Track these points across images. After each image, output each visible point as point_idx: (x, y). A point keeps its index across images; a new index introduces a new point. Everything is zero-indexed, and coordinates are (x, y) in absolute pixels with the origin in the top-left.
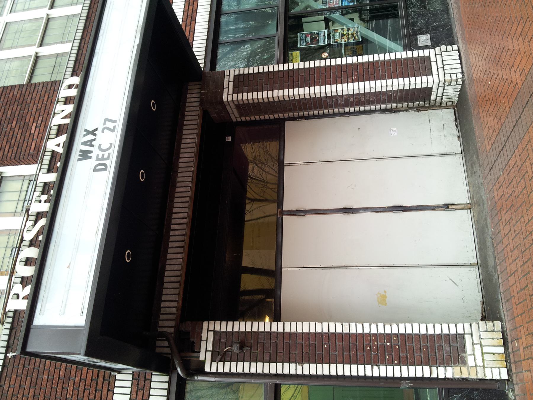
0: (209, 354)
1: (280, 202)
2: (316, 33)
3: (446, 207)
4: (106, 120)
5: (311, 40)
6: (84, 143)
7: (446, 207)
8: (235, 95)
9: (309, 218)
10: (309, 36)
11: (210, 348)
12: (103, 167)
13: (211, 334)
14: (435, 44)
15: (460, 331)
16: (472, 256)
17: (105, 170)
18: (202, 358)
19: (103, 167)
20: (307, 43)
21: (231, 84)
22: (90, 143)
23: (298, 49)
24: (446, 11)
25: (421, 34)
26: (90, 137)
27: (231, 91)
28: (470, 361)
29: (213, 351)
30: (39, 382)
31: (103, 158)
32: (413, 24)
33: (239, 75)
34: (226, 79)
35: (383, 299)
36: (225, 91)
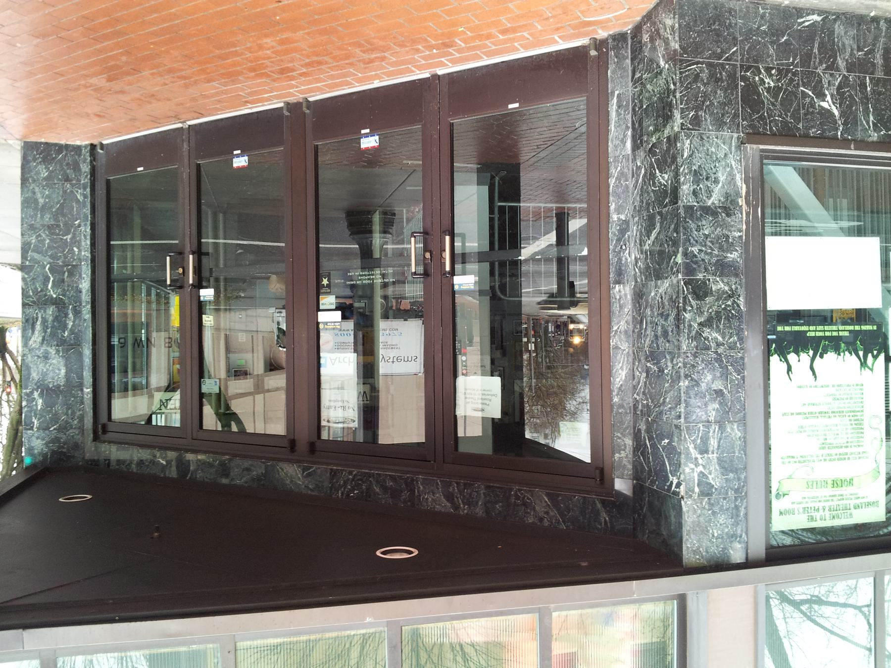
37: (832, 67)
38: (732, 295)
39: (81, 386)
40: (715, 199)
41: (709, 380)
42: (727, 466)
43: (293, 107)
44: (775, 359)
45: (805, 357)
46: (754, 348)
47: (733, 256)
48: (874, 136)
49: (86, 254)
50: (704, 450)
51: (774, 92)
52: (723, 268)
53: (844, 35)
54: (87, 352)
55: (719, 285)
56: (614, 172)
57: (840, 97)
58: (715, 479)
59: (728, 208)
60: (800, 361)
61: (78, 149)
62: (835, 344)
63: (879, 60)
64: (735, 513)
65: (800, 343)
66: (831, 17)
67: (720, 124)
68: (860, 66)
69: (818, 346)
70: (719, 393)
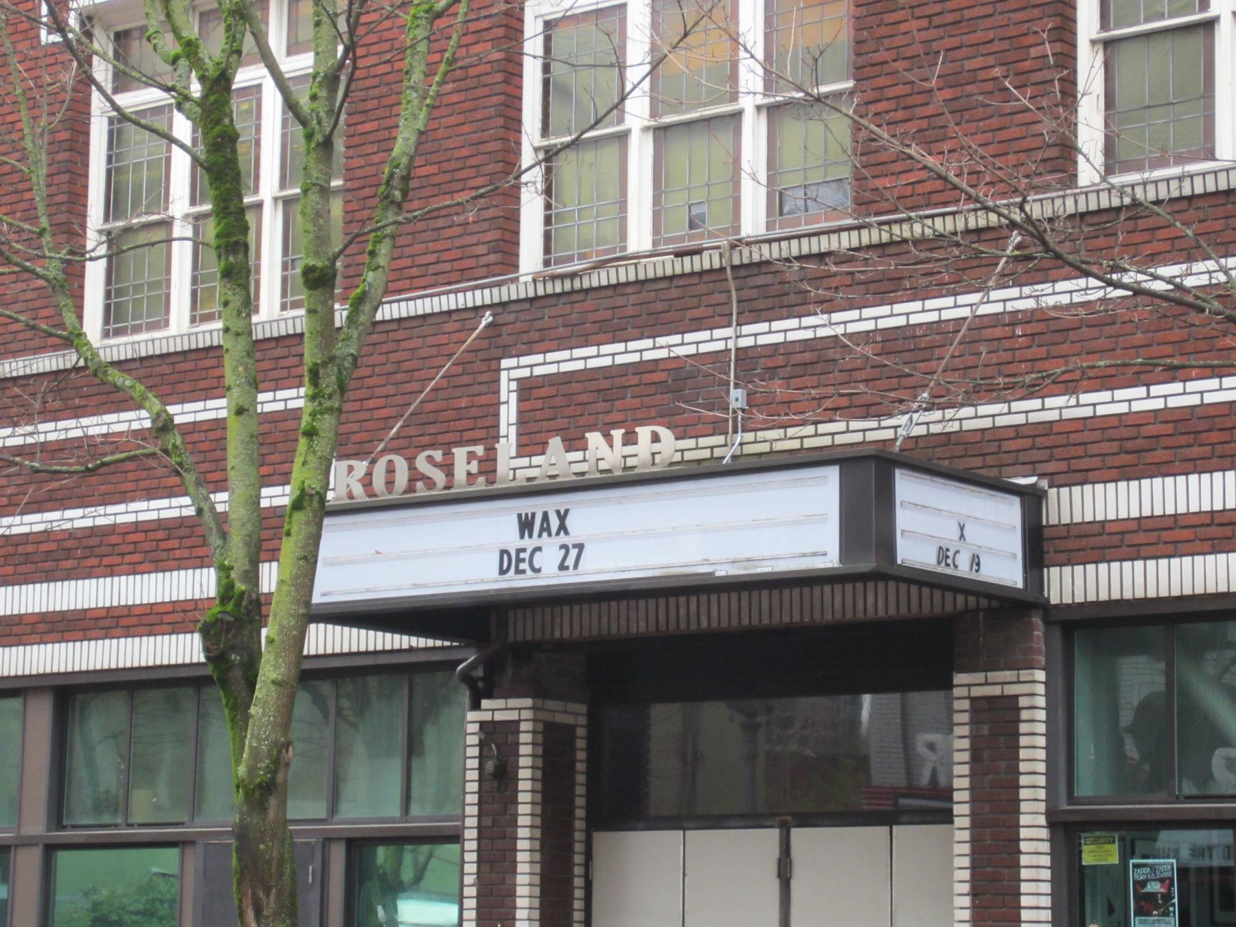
0: (487, 716)
1: (806, 820)
2: (1171, 909)
4: (580, 547)
5: (1152, 896)
6: (545, 517)
8: (966, 704)
9: (774, 885)
10: (1163, 890)
11: (499, 716)
12: (505, 566)
13: (513, 716)
17: (502, 572)
18: (485, 703)
19: (505, 566)
20: (1143, 883)
21: (995, 691)
22: (545, 528)
26: (554, 523)
27: (977, 692)
29: (493, 722)
30: (458, 392)
31: (519, 560)
33: (1018, 709)
34: (1009, 675)
36: (979, 677)
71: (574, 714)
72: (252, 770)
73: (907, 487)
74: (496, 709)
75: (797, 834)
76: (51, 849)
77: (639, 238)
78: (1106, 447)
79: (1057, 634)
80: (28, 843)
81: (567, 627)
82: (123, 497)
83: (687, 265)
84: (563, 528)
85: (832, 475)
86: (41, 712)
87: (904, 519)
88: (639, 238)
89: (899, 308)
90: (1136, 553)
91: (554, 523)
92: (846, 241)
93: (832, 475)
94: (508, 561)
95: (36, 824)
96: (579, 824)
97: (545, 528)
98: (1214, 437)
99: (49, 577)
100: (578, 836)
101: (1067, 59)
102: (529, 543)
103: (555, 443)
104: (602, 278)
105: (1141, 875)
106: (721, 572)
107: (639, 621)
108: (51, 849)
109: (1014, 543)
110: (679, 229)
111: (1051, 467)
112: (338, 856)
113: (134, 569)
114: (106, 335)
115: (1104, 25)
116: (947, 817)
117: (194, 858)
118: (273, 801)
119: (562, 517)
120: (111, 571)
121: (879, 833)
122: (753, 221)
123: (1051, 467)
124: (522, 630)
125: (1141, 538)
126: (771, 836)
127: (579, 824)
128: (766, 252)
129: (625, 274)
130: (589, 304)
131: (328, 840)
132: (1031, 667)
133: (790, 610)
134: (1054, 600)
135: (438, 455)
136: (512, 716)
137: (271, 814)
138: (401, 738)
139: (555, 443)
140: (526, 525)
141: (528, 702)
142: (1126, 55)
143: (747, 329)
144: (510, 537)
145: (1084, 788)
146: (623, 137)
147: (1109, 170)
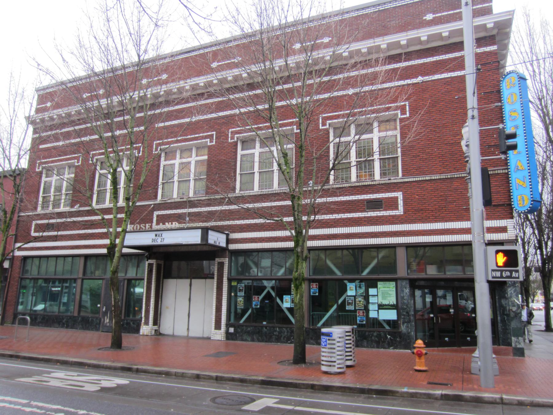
0: (149, 262)
1: (194, 278)
3: (188, 329)
7: (188, 329)
14: (227, 332)
15: (150, 325)
16: (176, 333)
21: (221, 261)
23: (237, 284)
24: (242, 340)
25: (234, 329)
26: (160, 235)
27: (219, 261)
28: (144, 326)
32: (238, 327)
35: (167, 308)
37: (388, 342)
38: (403, 312)
39: (499, 298)
40: (405, 324)
41: (406, 301)
42: (403, 291)
43: (459, 346)
44: (395, 303)
45: (391, 304)
46: (400, 305)
47: (403, 317)
48: (382, 333)
49: (499, 324)
50: (406, 293)
51: (397, 338)
52: (404, 315)
53: (386, 346)
54: (497, 305)
55: (404, 313)
56: (414, 330)
57: (387, 337)
58: (405, 289)
59: (403, 323)
60: (391, 303)
61: (503, 345)
62: (386, 305)
63: (381, 343)
64: (402, 285)
65: (391, 305)
66: (389, 348)
67: (405, 334)
68: (384, 342)
69: (388, 305)
70: (405, 300)
71: (162, 262)
72: (113, 269)
73: (210, 233)
74: (150, 261)
75: (193, 280)
76: (83, 279)
77: (175, 196)
78: (238, 228)
79: (230, 254)
80: (80, 278)
81: (161, 250)
82: (97, 228)
83: (182, 200)
84: (161, 236)
85: (200, 231)
86: (82, 260)
87: (210, 237)
88: (175, 196)
89: (211, 208)
90: (241, 243)
91: (160, 235)
92: (204, 198)
93: (200, 231)
94: (153, 240)
95: (81, 275)
96: (162, 278)
97: (159, 236)
98: (252, 228)
99: (85, 239)
100: (161, 280)
101: (235, 176)
102: (156, 238)
103: (161, 224)
104: (169, 201)
105: (240, 286)
106: (184, 243)
107: (172, 250)
108: (83, 279)
109: (225, 241)
110: (181, 195)
111: (231, 231)
112: (126, 282)
113: (98, 239)
114: (96, 205)
115: (240, 172)
116: (213, 278)
117: (104, 281)
118: (116, 274)
119: (161, 235)
120: (94, 239)
121: (204, 280)
122: (191, 194)
123: (231, 231)
124: (155, 250)
125: (242, 241)
126: (189, 280)
127: (162, 278)
128: (193, 199)
129: (173, 201)
130: (167, 205)
131: (124, 279)
132: (226, 258)
133: (193, 249)
134: (230, 249)
135: (144, 225)
136: (152, 262)
137: (116, 275)
138: (136, 264)
139: (161, 224)
140: (156, 235)
141: (155, 260)
142: (243, 177)
143: (189, 209)
144: (154, 237)
145: (232, 275)
146: (173, 182)
147: (240, 191)
